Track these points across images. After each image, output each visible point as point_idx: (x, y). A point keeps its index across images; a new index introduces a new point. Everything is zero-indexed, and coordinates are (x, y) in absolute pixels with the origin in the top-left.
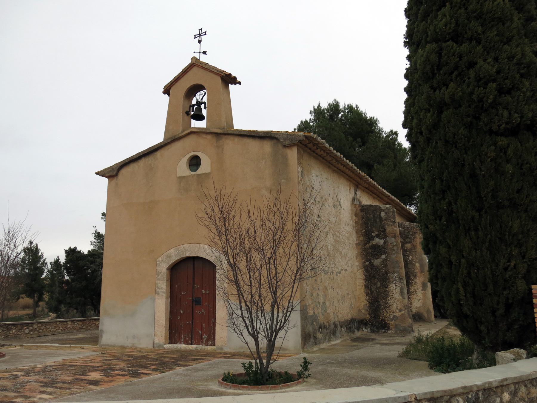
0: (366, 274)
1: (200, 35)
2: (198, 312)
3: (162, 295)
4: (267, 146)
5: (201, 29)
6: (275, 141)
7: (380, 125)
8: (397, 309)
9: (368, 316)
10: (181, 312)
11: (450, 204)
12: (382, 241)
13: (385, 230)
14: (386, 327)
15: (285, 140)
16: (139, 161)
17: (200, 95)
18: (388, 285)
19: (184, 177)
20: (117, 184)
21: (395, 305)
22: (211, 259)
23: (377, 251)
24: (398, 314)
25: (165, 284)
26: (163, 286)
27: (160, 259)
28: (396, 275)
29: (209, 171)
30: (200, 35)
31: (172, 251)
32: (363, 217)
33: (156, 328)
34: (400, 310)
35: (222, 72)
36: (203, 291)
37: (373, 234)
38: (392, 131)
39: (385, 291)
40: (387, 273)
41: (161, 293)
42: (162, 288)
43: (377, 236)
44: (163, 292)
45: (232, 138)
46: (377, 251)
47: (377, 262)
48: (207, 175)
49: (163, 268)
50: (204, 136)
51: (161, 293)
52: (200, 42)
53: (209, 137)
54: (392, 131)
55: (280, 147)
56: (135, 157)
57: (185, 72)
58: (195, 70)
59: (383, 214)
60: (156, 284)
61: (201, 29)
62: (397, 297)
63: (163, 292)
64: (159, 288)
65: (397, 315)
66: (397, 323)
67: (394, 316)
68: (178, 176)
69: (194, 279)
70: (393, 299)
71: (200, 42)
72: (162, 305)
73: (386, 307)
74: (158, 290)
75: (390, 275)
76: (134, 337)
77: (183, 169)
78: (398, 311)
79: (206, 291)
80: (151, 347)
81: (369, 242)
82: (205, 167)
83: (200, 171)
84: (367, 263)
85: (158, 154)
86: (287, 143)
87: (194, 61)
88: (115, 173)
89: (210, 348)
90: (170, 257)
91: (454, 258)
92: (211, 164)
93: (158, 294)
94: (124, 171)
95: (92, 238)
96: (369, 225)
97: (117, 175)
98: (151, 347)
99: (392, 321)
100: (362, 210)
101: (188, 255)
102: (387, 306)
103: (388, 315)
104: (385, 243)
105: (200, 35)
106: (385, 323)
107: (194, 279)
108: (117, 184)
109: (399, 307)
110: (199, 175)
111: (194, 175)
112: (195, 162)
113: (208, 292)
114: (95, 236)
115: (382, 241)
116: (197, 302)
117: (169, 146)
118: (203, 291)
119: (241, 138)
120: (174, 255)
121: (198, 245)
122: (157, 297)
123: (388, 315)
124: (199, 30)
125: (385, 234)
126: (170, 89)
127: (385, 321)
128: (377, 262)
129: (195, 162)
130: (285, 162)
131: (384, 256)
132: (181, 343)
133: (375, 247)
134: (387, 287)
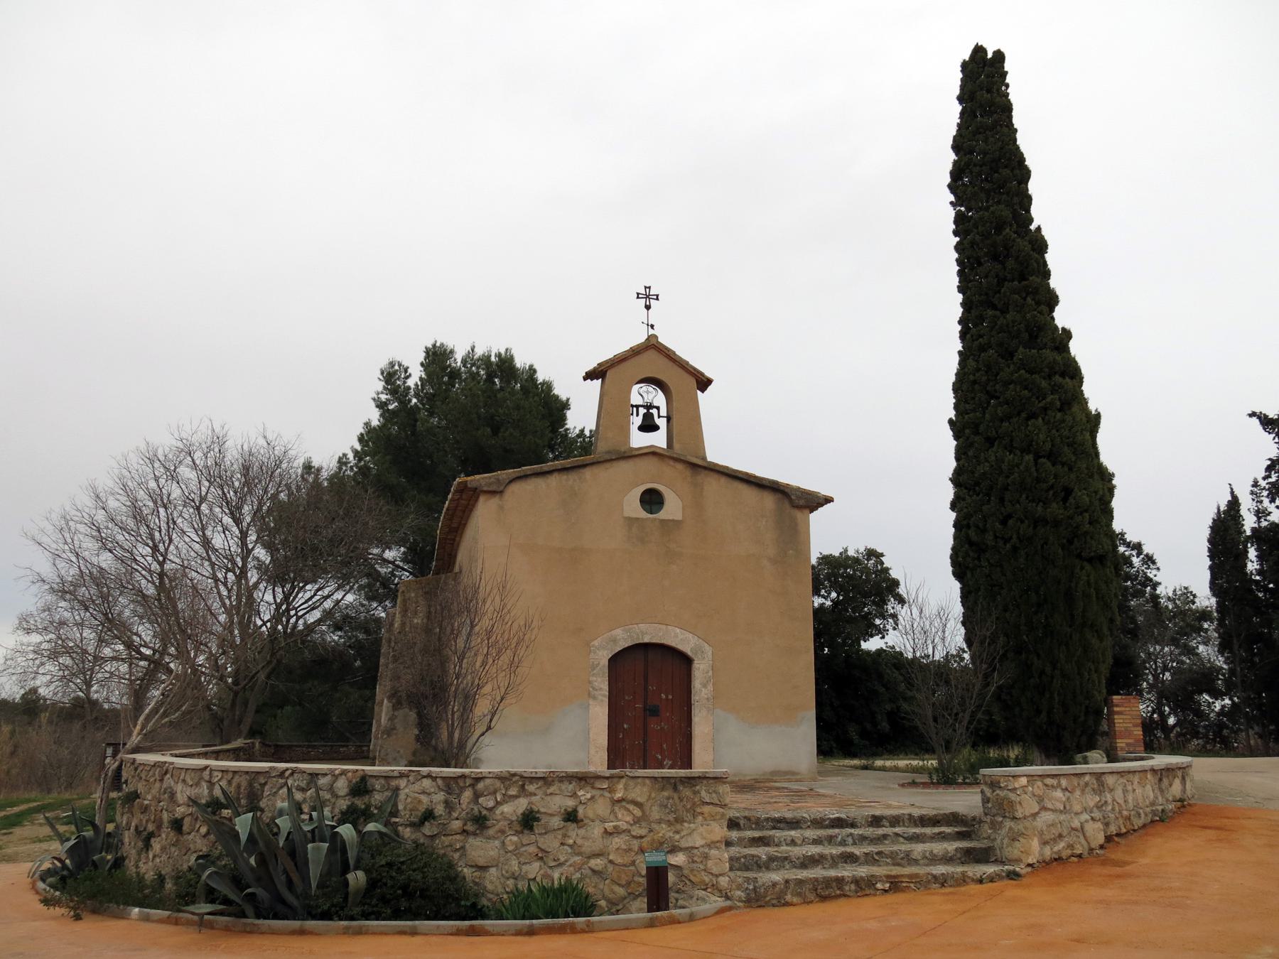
2: (654, 725)
4: (769, 500)
6: (780, 496)
7: (569, 414)
11: (1046, 618)
15: (799, 498)
20: (501, 508)
22: (686, 648)
26: (602, 684)
27: (596, 643)
29: (679, 517)
31: (618, 632)
33: (592, 751)
35: (702, 374)
36: (663, 696)
48: (677, 524)
49: (603, 657)
50: (671, 463)
52: (648, 307)
53: (680, 466)
57: (635, 352)
60: (590, 682)
68: (626, 514)
71: (648, 307)
72: (599, 714)
74: (593, 692)
77: (633, 507)
82: (673, 508)
83: (663, 515)
86: (802, 502)
90: (615, 641)
91: (1048, 669)
93: (594, 698)
97: (501, 492)
101: (646, 640)
108: (501, 508)
110: (662, 521)
112: (652, 500)
116: (653, 711)
117: (608, 465)
118: (663, 696)
119: (729, 480)
129: (652, 500)
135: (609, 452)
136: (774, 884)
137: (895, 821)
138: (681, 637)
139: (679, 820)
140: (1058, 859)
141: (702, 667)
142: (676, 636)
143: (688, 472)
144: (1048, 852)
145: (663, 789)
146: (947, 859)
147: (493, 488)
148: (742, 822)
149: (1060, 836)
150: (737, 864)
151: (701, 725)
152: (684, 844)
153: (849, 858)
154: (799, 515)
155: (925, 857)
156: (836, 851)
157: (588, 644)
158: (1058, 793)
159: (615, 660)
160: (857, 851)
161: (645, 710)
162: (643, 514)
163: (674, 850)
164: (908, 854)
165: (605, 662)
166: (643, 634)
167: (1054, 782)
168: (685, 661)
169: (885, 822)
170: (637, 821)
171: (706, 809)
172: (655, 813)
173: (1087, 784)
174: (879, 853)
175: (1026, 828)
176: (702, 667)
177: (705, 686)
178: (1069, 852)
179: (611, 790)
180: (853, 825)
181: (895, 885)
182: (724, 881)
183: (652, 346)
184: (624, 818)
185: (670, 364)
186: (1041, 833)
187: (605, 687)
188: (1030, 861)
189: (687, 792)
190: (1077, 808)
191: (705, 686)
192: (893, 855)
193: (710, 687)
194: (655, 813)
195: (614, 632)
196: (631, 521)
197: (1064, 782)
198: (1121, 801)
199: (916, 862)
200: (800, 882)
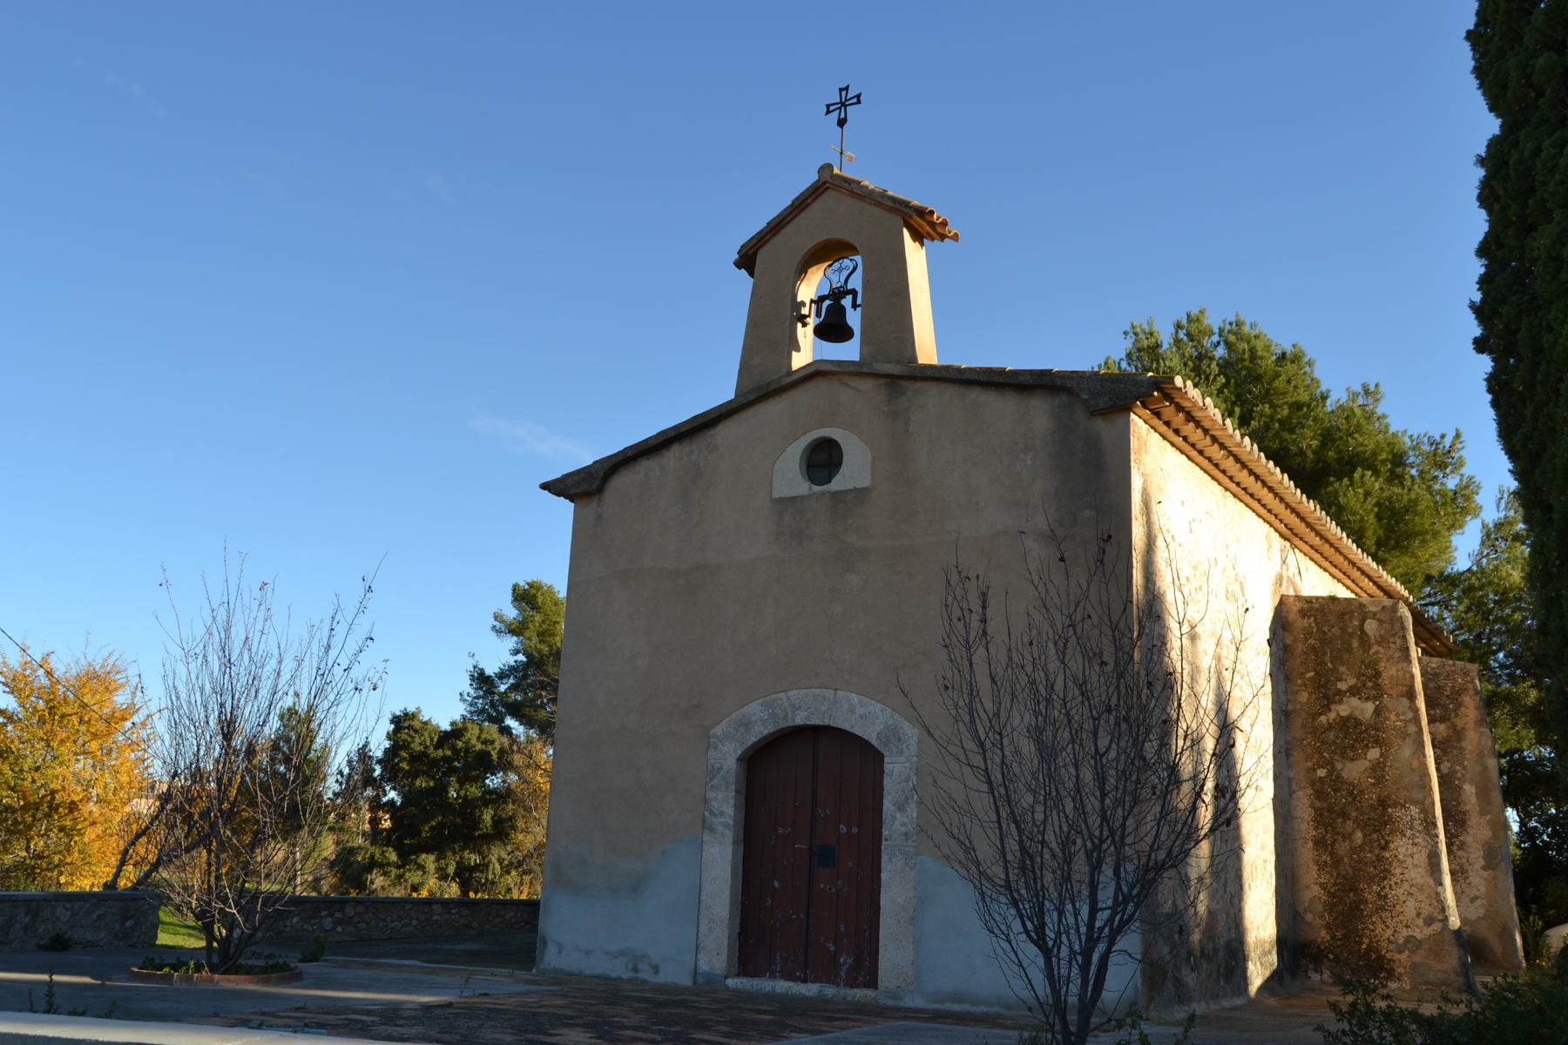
0: (1318, 804)
1: (843, 104)
3: (723, 835)
4: (1040, 410)
5: (847, 88)
6: (1065, 398)
8: (1418, 915)
9: (1323, 933)
10: (776, 884)
12: (1369, 707)
13: (1378, 674)
14: (1382, 969)
16: (665, 453)
17: (840, 270)
18: (1387, 842)
19: (793, 499)
21: (1411, 904)
22: (870, 734)
25: (732, 802)
26: (725, 805)
27: (718, 730)
28: (1414, 810)
29: (864, 481)
30: (843, 104)
31: (754, 709)
33: (703, 928)
37: (1342, 686)
39: (1380, 859)
40: (1383, 803)
41: (720, 829)
42: (722, 814)
43: (1354, 691)
44: (726, 826)
46: (1354, 735)
47: (1354, 770)
48: (860, 494)
49: (728, 756)
51: (720, 829)
52: (842, 123)
53: (867, 385)
56: (652, 443)
57: (800, 205)
58: (828, 199)
59: (1371, 626)
60: (706, 800)
61: (847, 88)
62: (1420, 881)
63: (726, 826)
64: (712, 814)
65: (1419, 936)
66: (1417, 959)
67: (1409, 939)
68: (776, 495)
70: (1406, 886)
71: (842, 123)
72: (719, 860)
73: (1382, 908)
77: (790, 479)
78: (1420, 922)
79: (849, 828)
80: (686, 981)
82: (854, 472)
83: (838, 483)
84: (1321, 773)
85: (722, 432)
86: (1103, 402)
87: (827, 177)
88: (595, 486)
89: (860, 994)
90: (746, 724)
92: (873, 462)
93: (712, 830)
94: (619, 482)
95: (466, 686)
96: (1327, 658)
97: (600, 490)
99: (1400, 952)
102: (1384, 905)
103: (1389, 932)
104: (1377, 711)
105: (843, 106)
106: (1381, 958)
110: (836, 495)
111: (823, 493)
112: (823, 459)
113: (855, 830)
114: (472, 678)
115: (1369, 707)
117: (749, 413)
120: (760, 720)
121: (829, 693)
122: (706, 837)
123: (1389, 932)
124: (841, 90)
125: (1377, 686)
126: (755, 254)
127: (1378, 952)
128: (1354, 770)
129: (823, 459)
131: (1374, 753)
132: (773, 976)
133: (1348, 725)
134: (1385, 848)
138: (860, 711)
141: (898, 768)
142: (852, 711)
147: (584, 488)
154: (1102, 427)
159: (763, 760)
162: (802, 487)
176: (898, 768)
177: (901, 808)
183: (828, 184)
191: (901, 808)
193: (912, 810)
195: (749, 709)
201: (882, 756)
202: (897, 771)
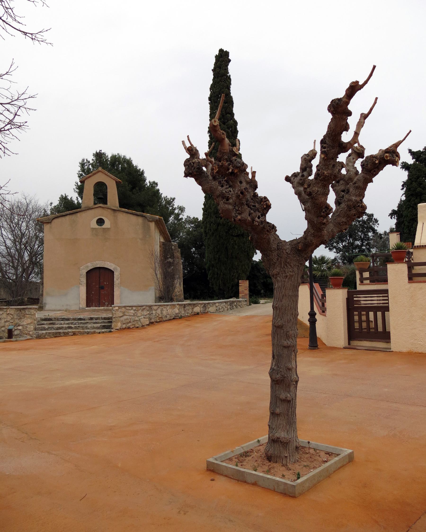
2: (103, 292)
11: (219, 256)
13: (173, 255)
15: (150, 218)
22: (112, 269)
23: (170, 264)
24: (178, 294)
26: (84, 280)
27: (82, 268)
29: (109, 227)
31: (89, 264)
32: (163, 248)
33: (81, 301)
34: (179, 292)
37: (168, 257)
38: (154, 182)
40: (174, 275)
43: (170, 258)
45: (122, 213)
46: (170, 264)
47: (170, 270)
48: (108, 229)
49: (84, 272)
50: (106, 209)
53: (109, 210)
54: (154, 182)
55: (147, 221)
59: (173, 247)
68: (91, 227)
69: (100, 278)
75: (175, 276)
76: (67, 305)
77: (94, 224)
80: (78, 309)
81: (166, 260)
82: (107, 224)
83: (104, 226)
86: (151, 220)
90: (88, 267)
91: (219, 272)
93: (81, 284)
97: (51, 222)
98: (78, 309)
100: (163, 245)
101: (98, 266)
107: (100, 278)
109: (179, 290)
111: (101, 228)
112: (100, 222)
116: (102, 288)
117: (85, 211)
120: (90, 266)
121: (104, 262)
128: (170, 270)
129: (100, 222)
130: (149, 228)
131: (172, 267)
133: (170, 263)
135: (85, 207)
136: (43, 334)
137: (97, 319)
139: (20, 318)
140: (129, 328)
142: (108, 265)
143: (112, 212)
144: (124, 326)
145: (18, 311)
146: (98, 328)
147: (48, 221)
148: (53, 319)
149: (130, 322)
150: (35, 329)
151: (117, 293)
152: (21, 324)
153: (71, 328)
155: (91, 327)
156: (67, 326)
157: (79, 268)
158: (132, 311)
159: (88, 273)
160: (73, 326)
161: (99, 288)
162: (97, 227)
163: (19, 325)
164: (86, 327)
165: (85, 273)
166: (97, 264)
167: (130, 308)
168: (111, 272)
169: (94, 319)
170: (12, 319)
171: (27, 316)
172: (15, 317)
173: (144, 309)
174: (79, 326)
175: (116, 320)
177: (117, 280)
178: (133, 326)
179: (6, 311)
180: (84, 320)
181: (74, 334)
182: (31, 333)
184: (9, 318)
185: (106, 176)
186: (122, 321)
187: (85, 281)
188: (117, 328)
189: (23, 312)
190: (139, 315)
191: (117, 280)
192: (82, 327)
193: (119, 280)
194: (15, 317)
196: (93, 229)
197: (134, 308)
198: (160, 313)
199: (89, 329)
200: (50, 333)
201: (113, 272)
202: (116, 274)
